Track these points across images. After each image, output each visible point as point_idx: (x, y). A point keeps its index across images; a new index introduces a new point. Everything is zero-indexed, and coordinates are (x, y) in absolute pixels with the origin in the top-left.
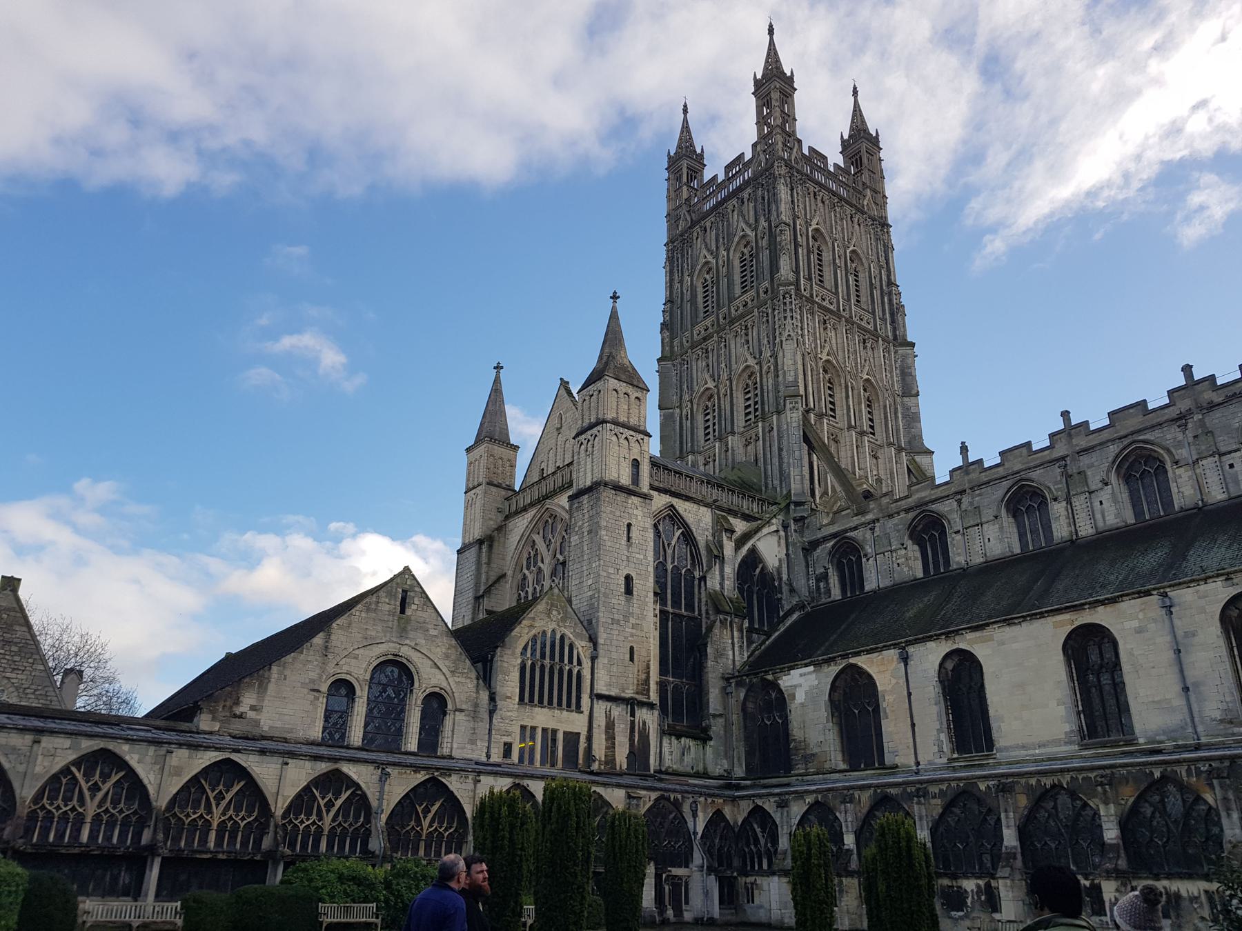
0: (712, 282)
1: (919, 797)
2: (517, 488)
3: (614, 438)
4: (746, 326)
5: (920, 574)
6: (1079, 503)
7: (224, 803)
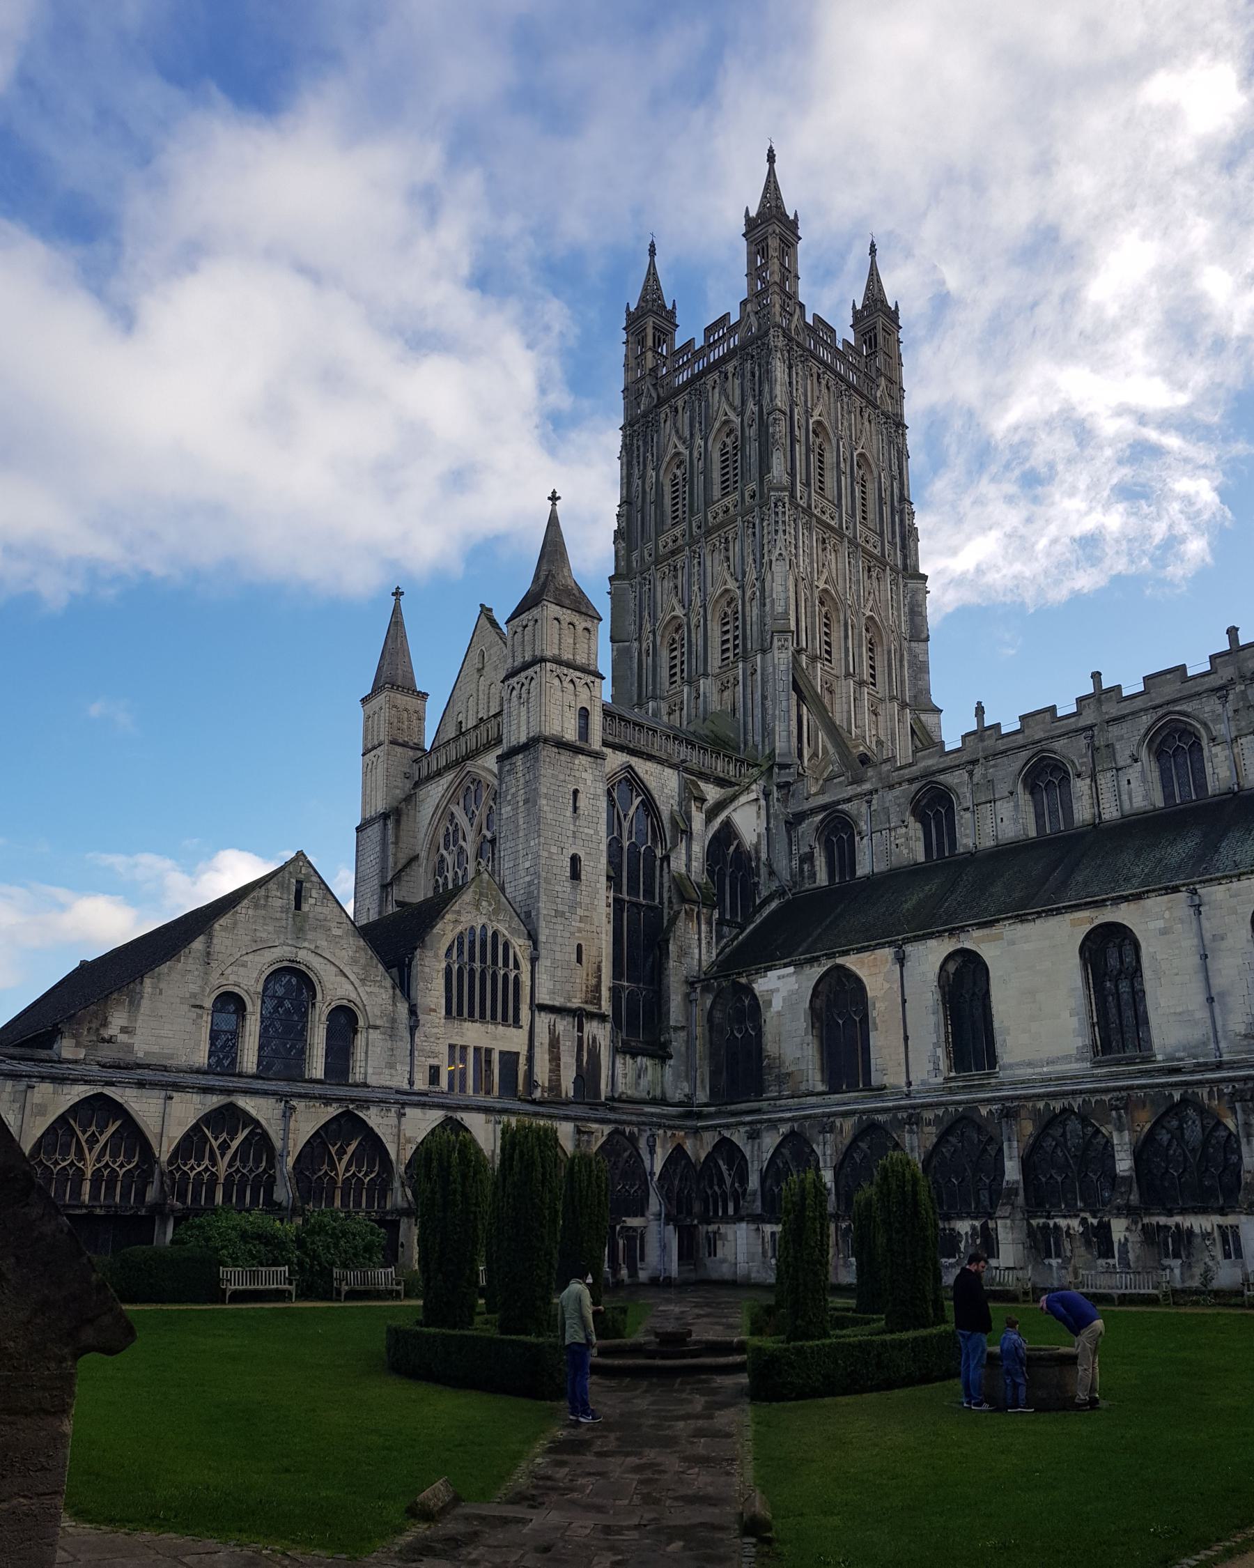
0: (684, 479)
1: (910, 1124)
7: (98, 1147)
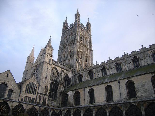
6: (110, 70)
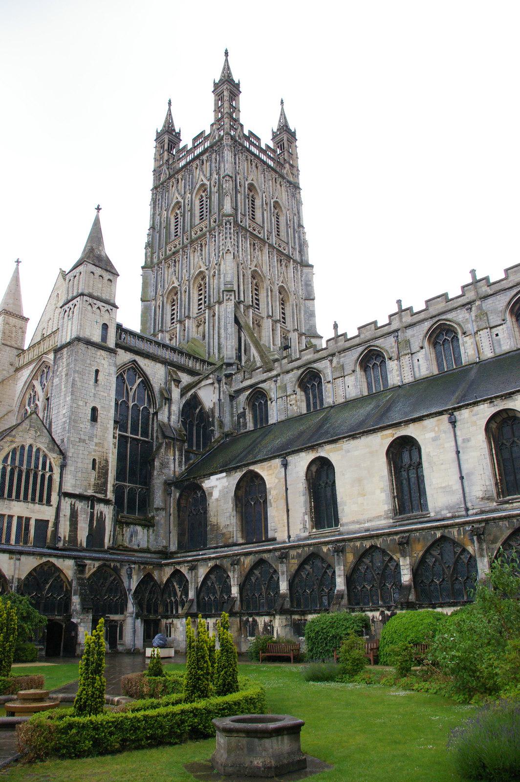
2: (26, 348)
3: (89, 307)
4: (201, 246)
5: (304, 411)
6: (405, 360)
